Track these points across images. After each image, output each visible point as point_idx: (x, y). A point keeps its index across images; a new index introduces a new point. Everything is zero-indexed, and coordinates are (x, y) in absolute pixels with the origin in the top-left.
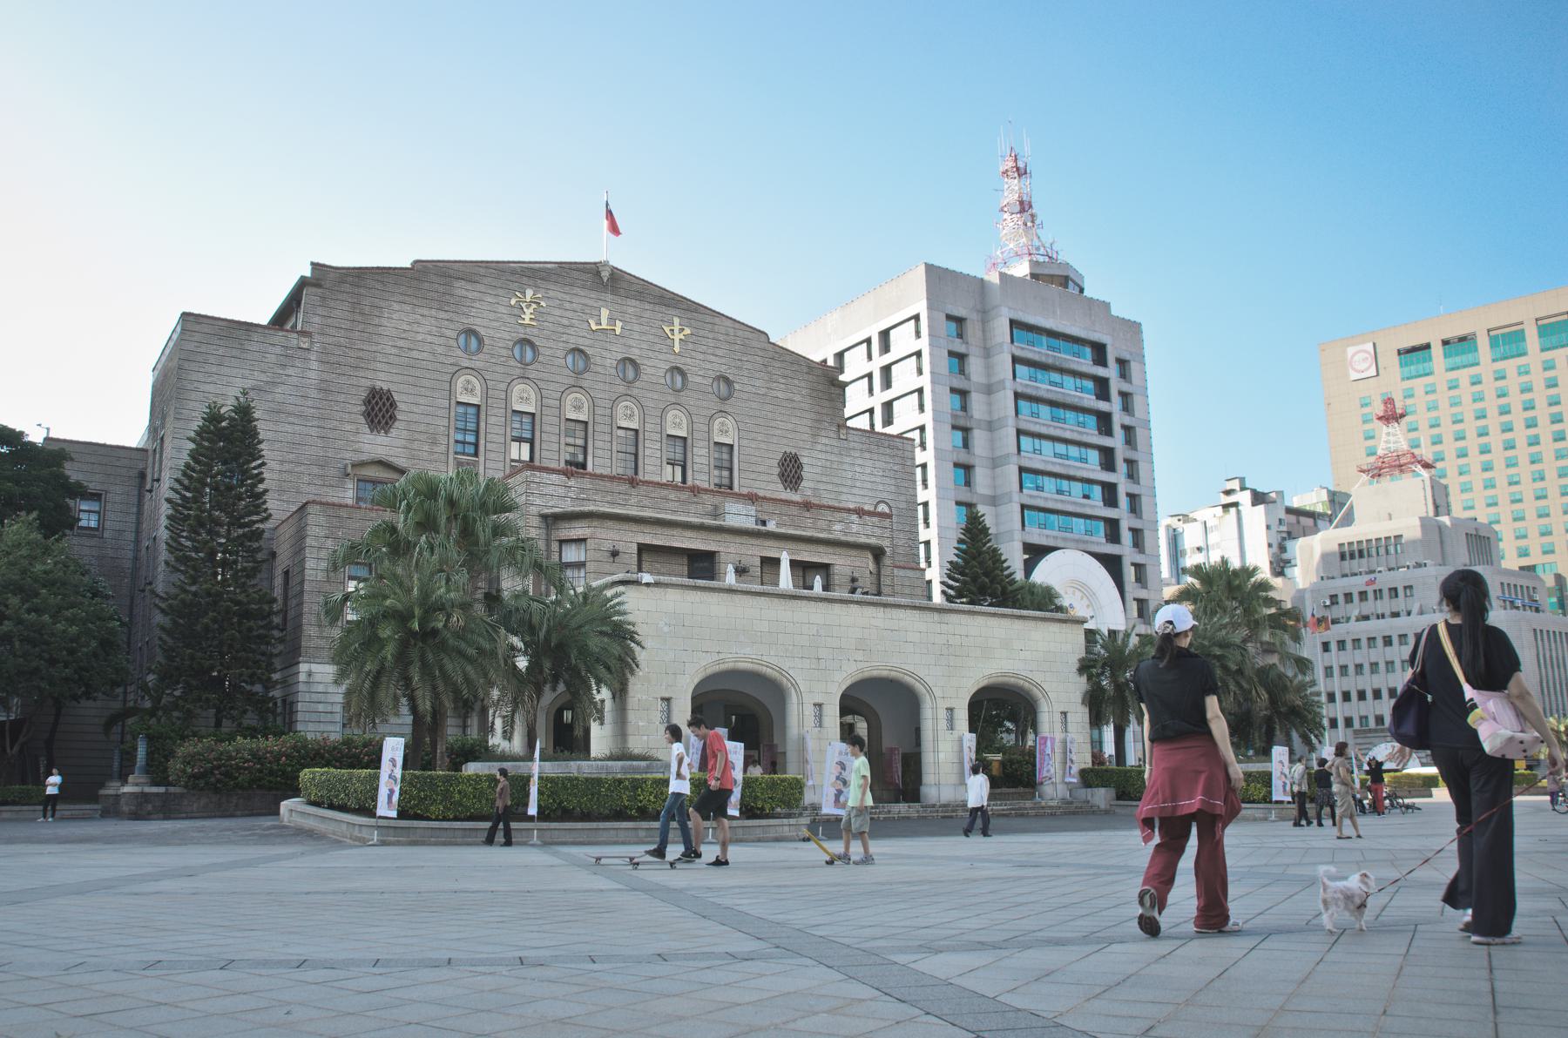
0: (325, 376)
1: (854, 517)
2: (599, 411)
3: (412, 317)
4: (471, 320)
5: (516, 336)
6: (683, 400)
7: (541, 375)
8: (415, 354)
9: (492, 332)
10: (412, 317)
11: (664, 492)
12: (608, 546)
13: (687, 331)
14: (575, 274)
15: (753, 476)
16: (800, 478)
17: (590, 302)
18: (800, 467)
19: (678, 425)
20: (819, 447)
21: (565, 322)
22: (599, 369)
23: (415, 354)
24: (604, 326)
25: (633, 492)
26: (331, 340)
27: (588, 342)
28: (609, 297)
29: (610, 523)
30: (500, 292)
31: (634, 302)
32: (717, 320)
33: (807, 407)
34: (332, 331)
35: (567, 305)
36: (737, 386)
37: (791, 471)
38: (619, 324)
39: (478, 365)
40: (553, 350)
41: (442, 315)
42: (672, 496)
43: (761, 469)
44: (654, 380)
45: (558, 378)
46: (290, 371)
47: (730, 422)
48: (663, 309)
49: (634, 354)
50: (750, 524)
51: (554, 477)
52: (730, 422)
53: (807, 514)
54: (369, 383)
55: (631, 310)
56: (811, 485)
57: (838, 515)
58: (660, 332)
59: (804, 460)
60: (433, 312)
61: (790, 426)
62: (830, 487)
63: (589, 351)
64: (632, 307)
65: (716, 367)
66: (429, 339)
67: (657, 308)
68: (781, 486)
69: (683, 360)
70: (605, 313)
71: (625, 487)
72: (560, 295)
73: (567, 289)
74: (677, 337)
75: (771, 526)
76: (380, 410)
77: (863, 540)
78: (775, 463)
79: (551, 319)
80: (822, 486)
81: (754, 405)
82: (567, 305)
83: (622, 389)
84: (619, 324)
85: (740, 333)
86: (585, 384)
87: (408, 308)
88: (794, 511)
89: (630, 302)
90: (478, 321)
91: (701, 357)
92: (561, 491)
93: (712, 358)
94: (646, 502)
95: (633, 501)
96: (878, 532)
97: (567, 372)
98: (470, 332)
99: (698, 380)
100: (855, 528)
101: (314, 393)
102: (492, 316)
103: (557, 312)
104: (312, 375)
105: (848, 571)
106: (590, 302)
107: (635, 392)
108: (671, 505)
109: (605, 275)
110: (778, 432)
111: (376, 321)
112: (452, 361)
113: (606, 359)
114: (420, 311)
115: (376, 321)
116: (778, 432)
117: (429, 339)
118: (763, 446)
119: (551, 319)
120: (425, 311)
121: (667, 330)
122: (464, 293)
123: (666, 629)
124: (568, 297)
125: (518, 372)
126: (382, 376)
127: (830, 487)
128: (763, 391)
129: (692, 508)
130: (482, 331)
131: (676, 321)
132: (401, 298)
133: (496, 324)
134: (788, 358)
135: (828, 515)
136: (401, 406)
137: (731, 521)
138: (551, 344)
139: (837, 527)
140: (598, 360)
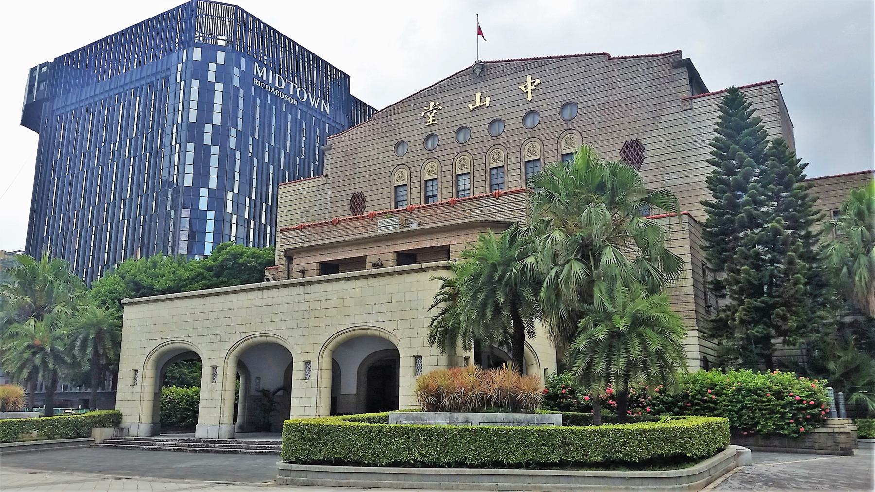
0: (333, 195)
1: (492, 201)
2: (476, 162)
3: (371, 147)
4: (401, 136)
5: (425, 135)
6: (537, 133)
7: (443, 153)
8: (374, 167)
9: (411, 138)
10: (371, 147)
12: (301, 267)
13: (538, 81)
14: (460, 79)
16: (642, 158)
17: (469, 93)
18: (642, 149)
19: (531, 153)
20: (661, 126)
21: (454, 113)
22: (476, 135)
23: (374, 167)
24: (478, 104)
25: (335, 228)
26: (335, 175)
27: (469, 120)
28: (478, 85)
29: (303, 255)
30: (417, 112)
31: (501, 79)
32: (563, 63)
33: (648, 96)
34: (336, 170)
35: (455, 102)
36: (580, 106)
38: (488, 99)
39: (406, 160)
40: (446, 134)
41: (386, 139)
44: (514, 127)
45: (451, 151)
46: (319, 198)
47: (576, 136)
48: (520, 74)
49: (500, 115)
50: (396, 229)
51: (294, 233)
52: (576, 136)
53: (452, 210)
54: (352, 192)
55: (497, 86)
56: (654, 159)
58: (518, 92)
60: (382, 140)
61: (631, 118)
63: (469, 126)
64: (497, 84)
65: (562, 98)
66: (380, 155)
67: (516, 76)
69: (536, 104)
70: (478, 95)
71: (331, 227)
72: (450, 98)
73: (455, 92)
74: (530, 87)
75: (414, 226)
76: (357, 203)
77: (500, 218)
78: (617, 153)
79: (446, 115)
81: (597, 114)
82: (455, 102)
83: (492, 143)
84: (488, 99)
85: (582, 64)
86: (467, 148)
87: (369, 143)
88: (442, 210)
89: (496, 81)
90: (405, 135)
91: (550, 95)
92: (297, 240)
93: (559, 93)
94: (343, 233)
97: (457, 145)
98: (401, 143)
99: (548, 113)
101: (328, 206)
102: (412, 128)
103: (449, 109)
104: (328, 196)
105: (461, 247)
106: (469, 93)
107: (500, 141)
108: (357, 231)
109: (478, 71)
110: (617, 128)
111: (355, 156)
112: (391, 163)
113: (480, 127)
114: (375, 142)
115: (355, 156)
116: (617, 128)
117: (380, 155)
119: (446, 115)
120: (378, 141)
121: (522, 87)
122: (397, 121)
124: (455, 97)
125: (427, 156)
126: (358, 185)
128: (604, 100)
130: (406, 140)
131: (529, 78)
132: (366, 139)
133: (414, 132)
134: (628, 64)
136: (367, 199)
137: (381, 231)
138: (447, 131)
140: (476, 129)
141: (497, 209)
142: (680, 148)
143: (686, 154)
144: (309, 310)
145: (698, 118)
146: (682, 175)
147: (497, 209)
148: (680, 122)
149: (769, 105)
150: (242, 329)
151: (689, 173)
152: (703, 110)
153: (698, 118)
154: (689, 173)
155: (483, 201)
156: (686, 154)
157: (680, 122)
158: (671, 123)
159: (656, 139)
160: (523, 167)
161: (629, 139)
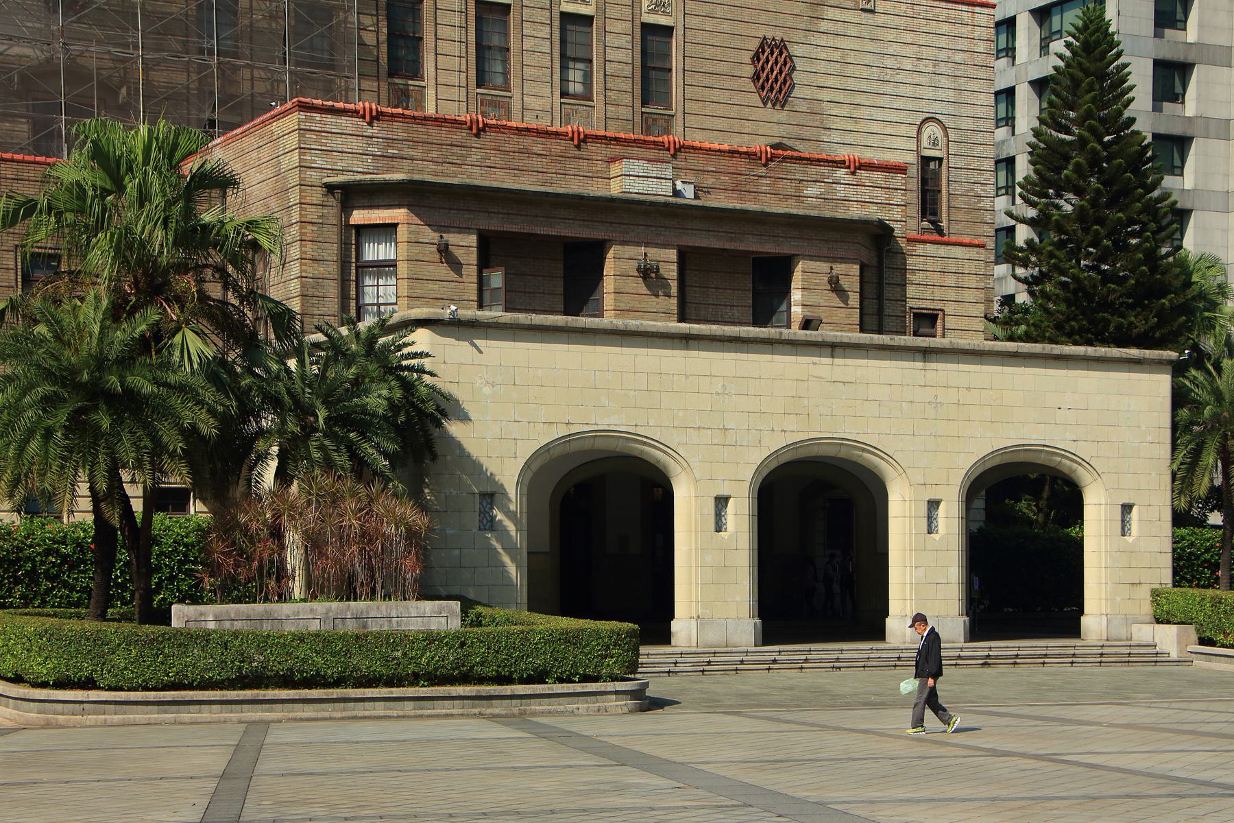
11: (527, 141)
15: (706, 80)
20: (823, 26)
25: (474, 142)
37: (773, 72)
42: (537, 149)
43: (722, 68)
57: (813, 170)
59: (795, 50)
62: (840, 97)
68: (755, 99)
71: (460, 136)
77: (856, 212)
78: (747, 57)
80: (825, 95)
92: (356, 144)
94: (495, 159)
95: (475, 157)
96: (881, 195)
100: (841, 191)
108: (537, 163)
118: (725, 27)
123: (487, 390)
127: (840, 97)
129: (571, 166)
135: (797, 171)
139: (813, 190)
141: (851, 193)
142: (852, 84)
143: (859, 99)
144: (937, 404)
145: (881, 34)
146: (849, 138)
147: (851, 193)
148: (852, 31)
149: (982, 47)
150: (790, 423)
151: (861, 139)
152: (889, 20)
153: (881, 34)
154: (861, 139)
155: (825, 170)
156: (859, 99)
157: (852, 31)
158: (839, 28)
159: (815, 52)
160: (557, 23)
161: (769, 35)
